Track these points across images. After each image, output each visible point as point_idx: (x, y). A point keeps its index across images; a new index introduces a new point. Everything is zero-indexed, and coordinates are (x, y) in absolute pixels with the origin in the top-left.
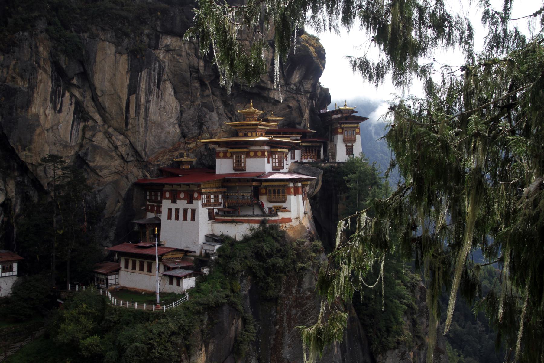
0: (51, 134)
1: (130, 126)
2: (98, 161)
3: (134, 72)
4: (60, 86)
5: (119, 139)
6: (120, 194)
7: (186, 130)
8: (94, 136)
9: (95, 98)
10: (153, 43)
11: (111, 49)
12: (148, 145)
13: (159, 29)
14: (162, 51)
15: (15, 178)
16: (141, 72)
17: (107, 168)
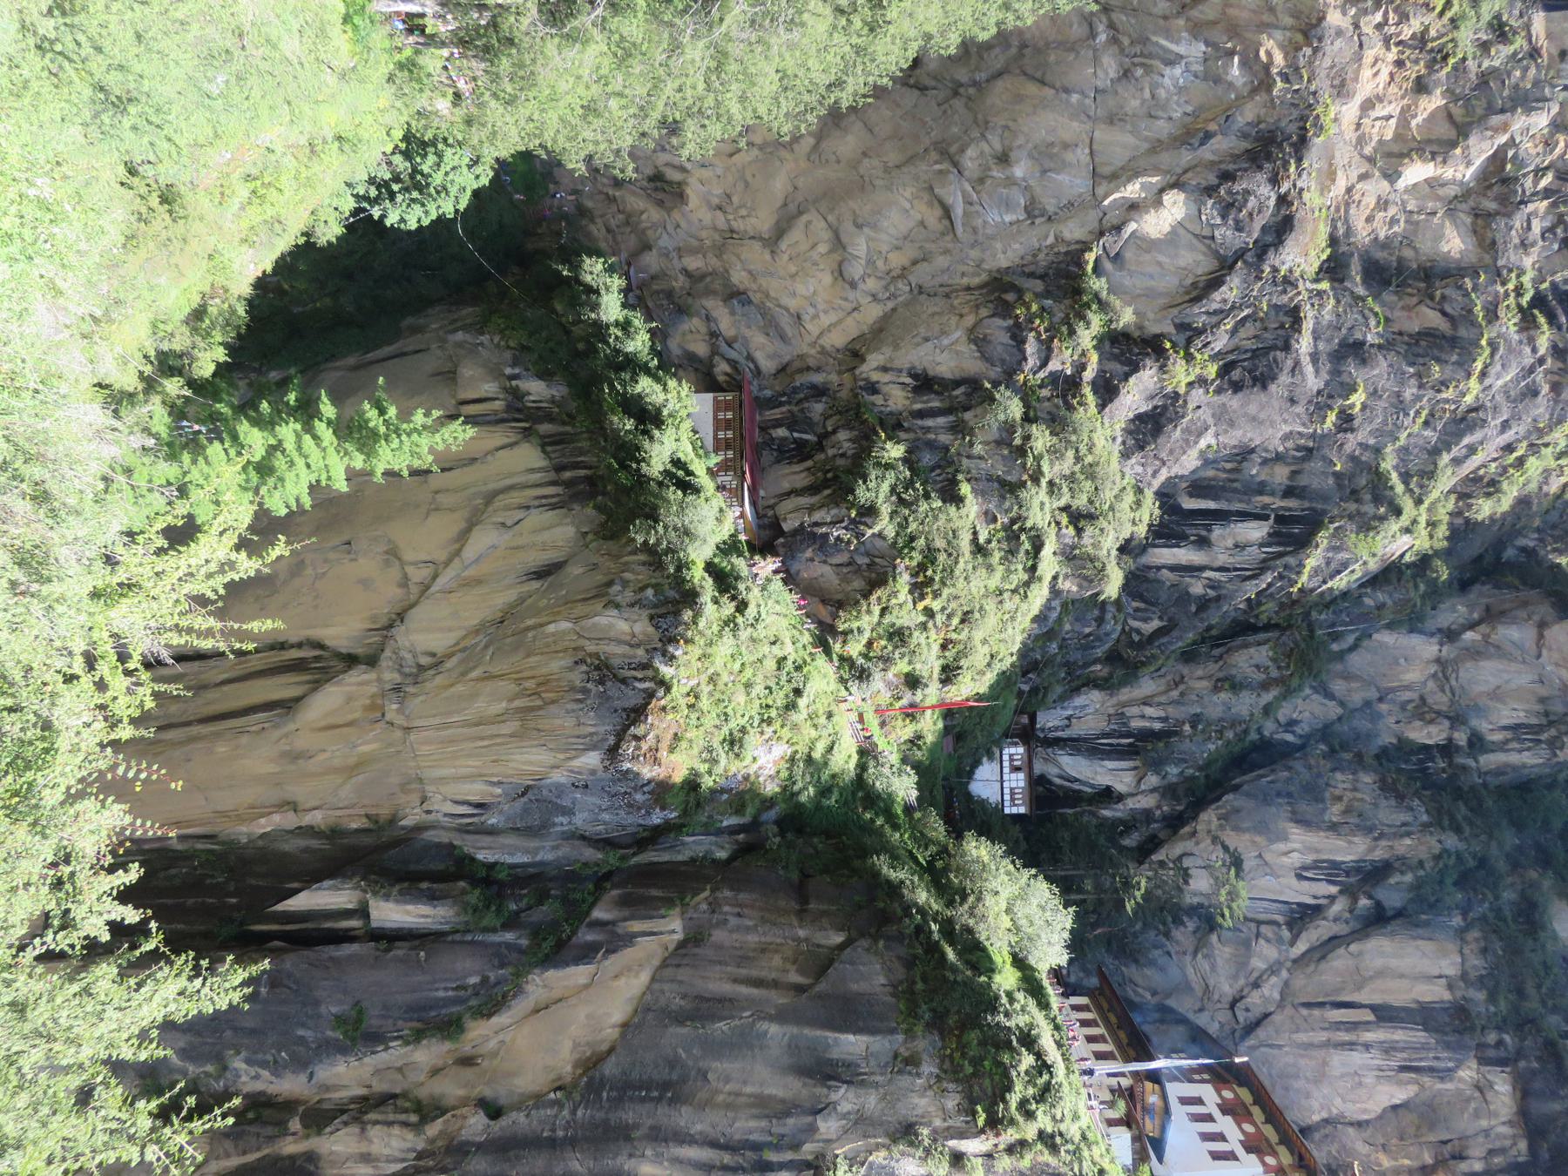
0: (1254, 863)
1: (1305, 1012)
2: (1222, 951)
3: (1423, 1016)
4: (1348, 874)
5: (1271, 989)
6: (1168, 995)
7: (1317, 1136)
8: (1268, 941)
9: (1333, 942)
10: (1491, 1053)
11: (1449, 965)
12: (1275, 1052)
13: (1522, 1064)
14: (1474, 1075)
15: (1159, 807)
16: (1425, 1030)
17: (1213, 967)
